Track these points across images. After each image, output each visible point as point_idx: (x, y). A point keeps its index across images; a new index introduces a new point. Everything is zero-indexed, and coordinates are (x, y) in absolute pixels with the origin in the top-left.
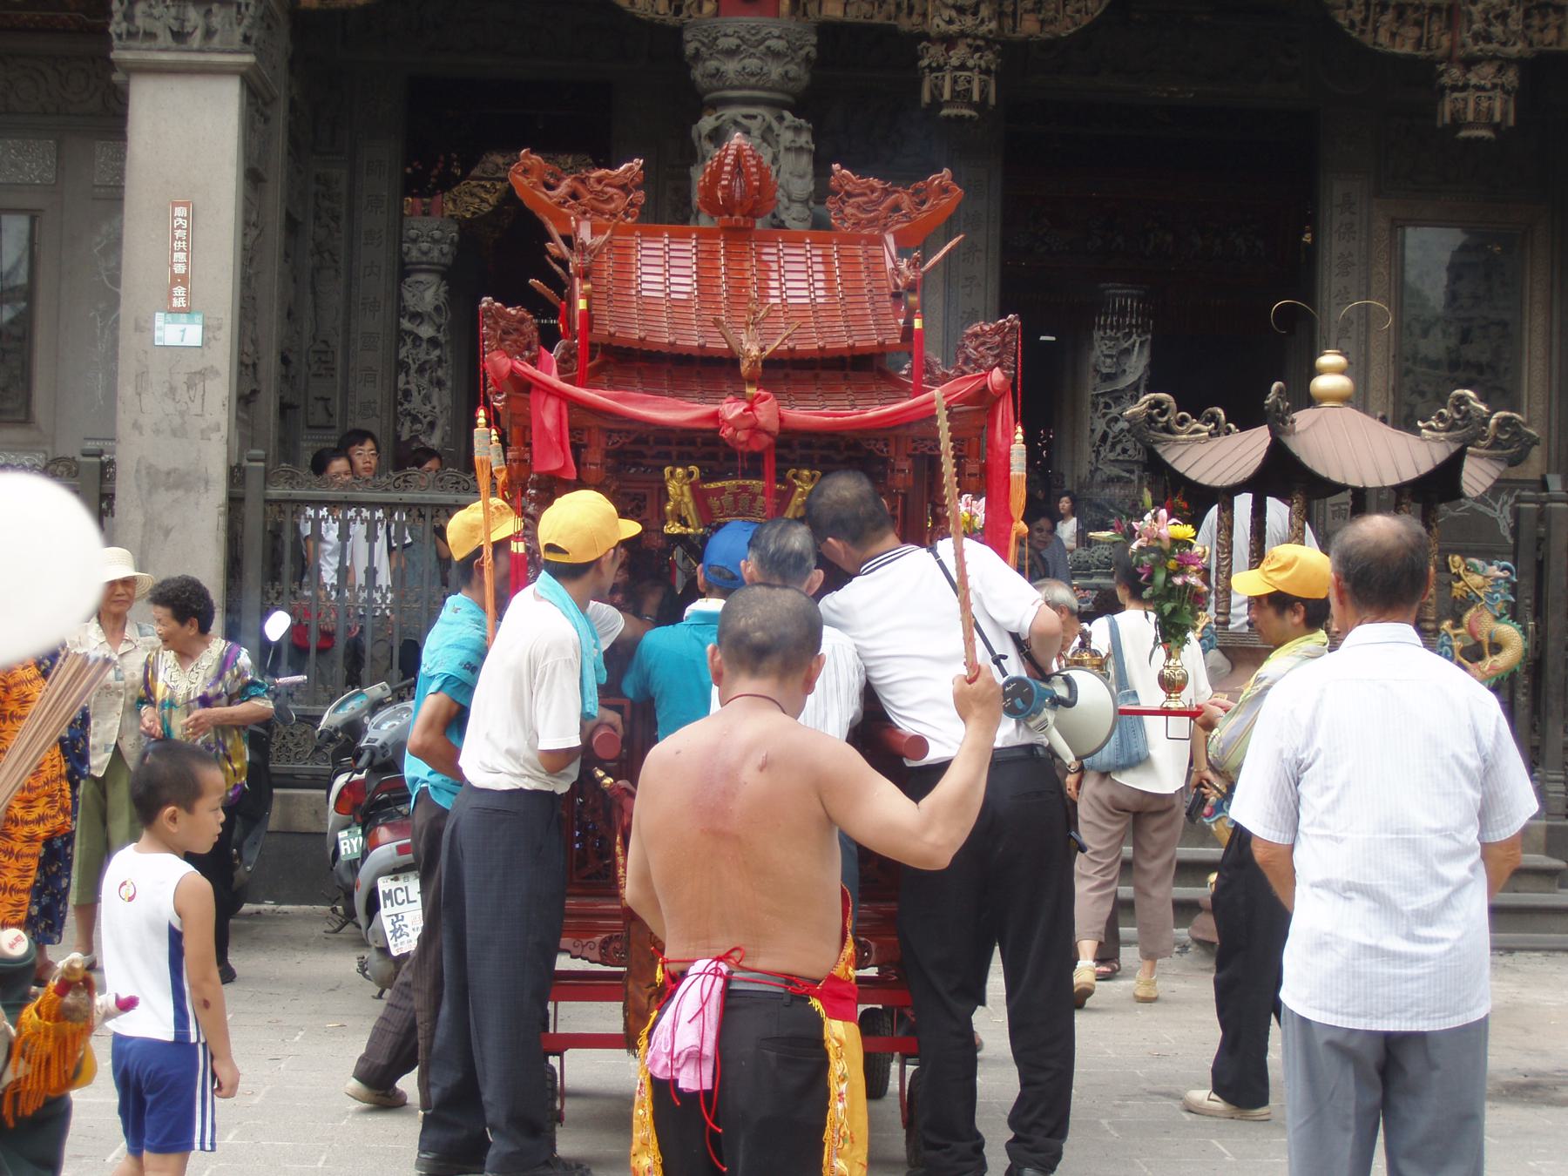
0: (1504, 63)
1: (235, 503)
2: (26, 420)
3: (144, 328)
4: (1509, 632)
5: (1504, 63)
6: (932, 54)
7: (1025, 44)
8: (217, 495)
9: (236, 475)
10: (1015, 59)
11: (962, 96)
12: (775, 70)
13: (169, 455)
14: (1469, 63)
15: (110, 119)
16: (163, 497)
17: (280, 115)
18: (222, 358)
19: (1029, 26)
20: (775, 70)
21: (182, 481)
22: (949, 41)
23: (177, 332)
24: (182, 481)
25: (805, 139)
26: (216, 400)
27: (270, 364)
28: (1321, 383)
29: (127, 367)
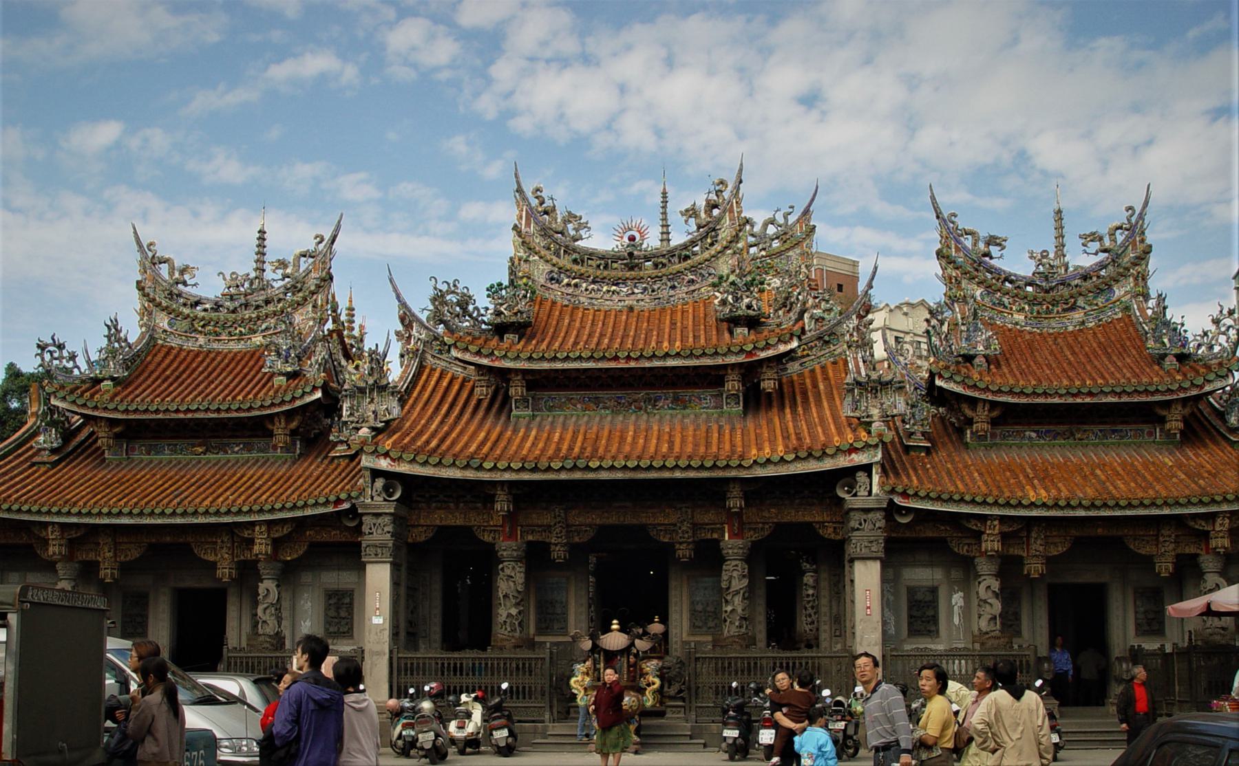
0: (689, 543)
1: (391, 658)
2: (351, 637)
3: (370, 619)
4: (658, 682)
5: (689, 543)
6: (553, 547)
7: (577, 544)
8: (387, 656)
9: (391, 652)
10: (573, 548)
11: (559, 557)
12: (515, 554)
13: (377, 648)
14: (681, 543)
15: (365, 569)
16: (375, 658)
17: (403, 569)
18: (387, 626)
19: (577, 539)
20: (515, 554)
21: (378, 653)
22: (556, 545)
23: (377, 620)
24: (378, 653)
25: (523, 569)
26: (386, 636)
27: (402, 625)
28: (614, 627)
29: (367, 629)
